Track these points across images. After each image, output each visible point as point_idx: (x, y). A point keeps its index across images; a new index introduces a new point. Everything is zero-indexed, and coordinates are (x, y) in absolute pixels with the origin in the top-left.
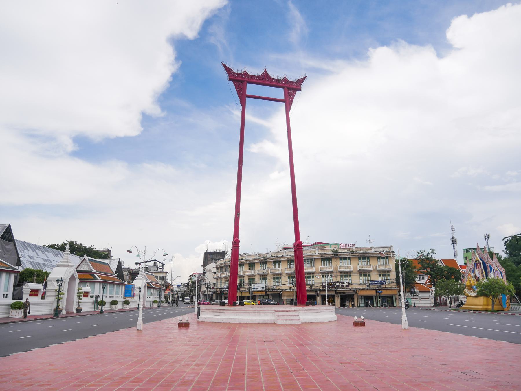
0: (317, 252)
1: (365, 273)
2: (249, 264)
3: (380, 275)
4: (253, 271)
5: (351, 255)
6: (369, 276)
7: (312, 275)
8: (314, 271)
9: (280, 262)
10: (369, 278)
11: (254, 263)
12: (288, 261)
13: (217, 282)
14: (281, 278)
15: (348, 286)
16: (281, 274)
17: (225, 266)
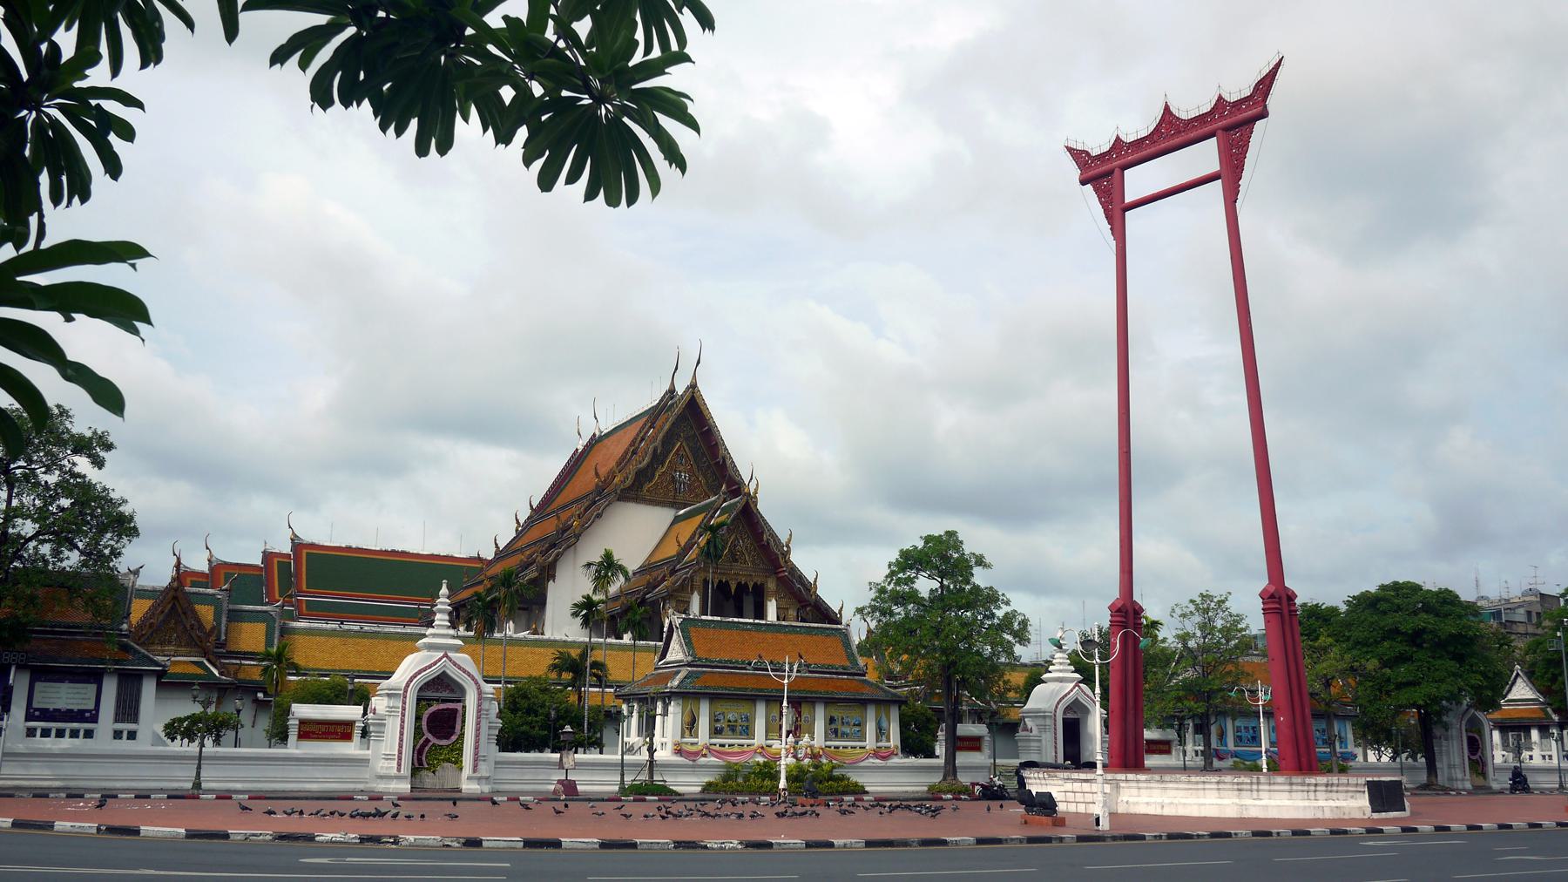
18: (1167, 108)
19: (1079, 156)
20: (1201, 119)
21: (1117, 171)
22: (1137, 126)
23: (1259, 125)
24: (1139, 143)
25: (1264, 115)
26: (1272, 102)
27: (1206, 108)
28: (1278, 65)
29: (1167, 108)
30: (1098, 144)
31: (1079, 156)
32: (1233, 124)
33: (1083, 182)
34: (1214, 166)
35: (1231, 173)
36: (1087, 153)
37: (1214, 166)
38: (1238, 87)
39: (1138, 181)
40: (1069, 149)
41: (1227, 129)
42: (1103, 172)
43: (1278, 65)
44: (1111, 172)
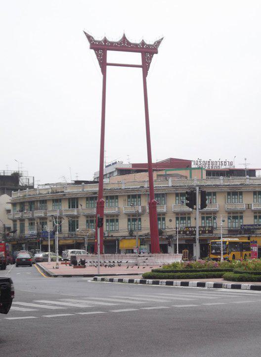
0: (170, 184)
1: (235, 215)
2: (69, 199)
3: (255, 217)
4: (76, 210)
5: (215, 190)
6: (241, 218)
7: (161, 217)
8: (165, 210)
9: (117, 197)
10: (241, 221)
11: (77, 199)
12: (129, 197)
13: (15, 225)
14: (117, 220)
15: (211, 232)
16: (117, 215)
17: (29, 202)
19: (89, 38)
20: (136, 45)
22: (115, 38)
23: (155, 55)
24: (112, 43)
26: (159, 49)
28: (162, 39)
30: (98, 37)
31: (89, 38)
32: (148, 51)
33: (91, 48)
34: (140, 64)
35: (145, 67)
36: (92, 38)
37: (140, 64)
38: (150, 41)
39: (112, 56)
40: (85, 33)
42: (101, 48)
43: (162, 39)
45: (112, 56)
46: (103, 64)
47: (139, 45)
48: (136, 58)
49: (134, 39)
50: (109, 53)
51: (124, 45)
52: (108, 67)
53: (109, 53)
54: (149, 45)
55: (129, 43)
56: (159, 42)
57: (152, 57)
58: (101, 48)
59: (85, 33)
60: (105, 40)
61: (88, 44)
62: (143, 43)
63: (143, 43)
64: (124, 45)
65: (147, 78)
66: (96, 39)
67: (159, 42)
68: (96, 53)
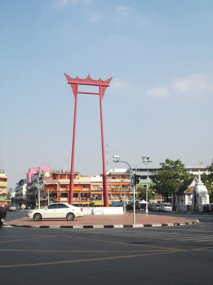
18: (89, 76)
20: (96, 81)
21: (78, 84)
22: (83, 76)
24: (81, 80)
25: (109, 86)
26: (110, 84)
27: (97, 80)
28: (111, 78)
29: (89, 76)
30: (73, 76)
33: (69, 83)
34: (99, 92)
35: (101, 94)
38: (104, 79)
39: (81, 88)
40: (65, 75)
41: (102, 86)
42: (74, 83)
43: (111, 78)
44: (76, 84)
45: (81, 88)
46: (76, 92)
47: (97, 81)
48: (96, 89)
49: (95, 78)
50: (80, 86)
51: (89, 82)
52: (79, 95)
53: (80, 86)
54: (104, 82)
55: (92, 80)
56: (109, 80)
57: (106, 88)
58: (74, 83)
59: (65, 75)
60: (77, 79)
61: (66, 81)
62: (100, 80)
63: (100, 80)
64: (89, 82)
65: (102, 101)
66: (71, 78)
67: (109, 80)
68: (71, 86)
